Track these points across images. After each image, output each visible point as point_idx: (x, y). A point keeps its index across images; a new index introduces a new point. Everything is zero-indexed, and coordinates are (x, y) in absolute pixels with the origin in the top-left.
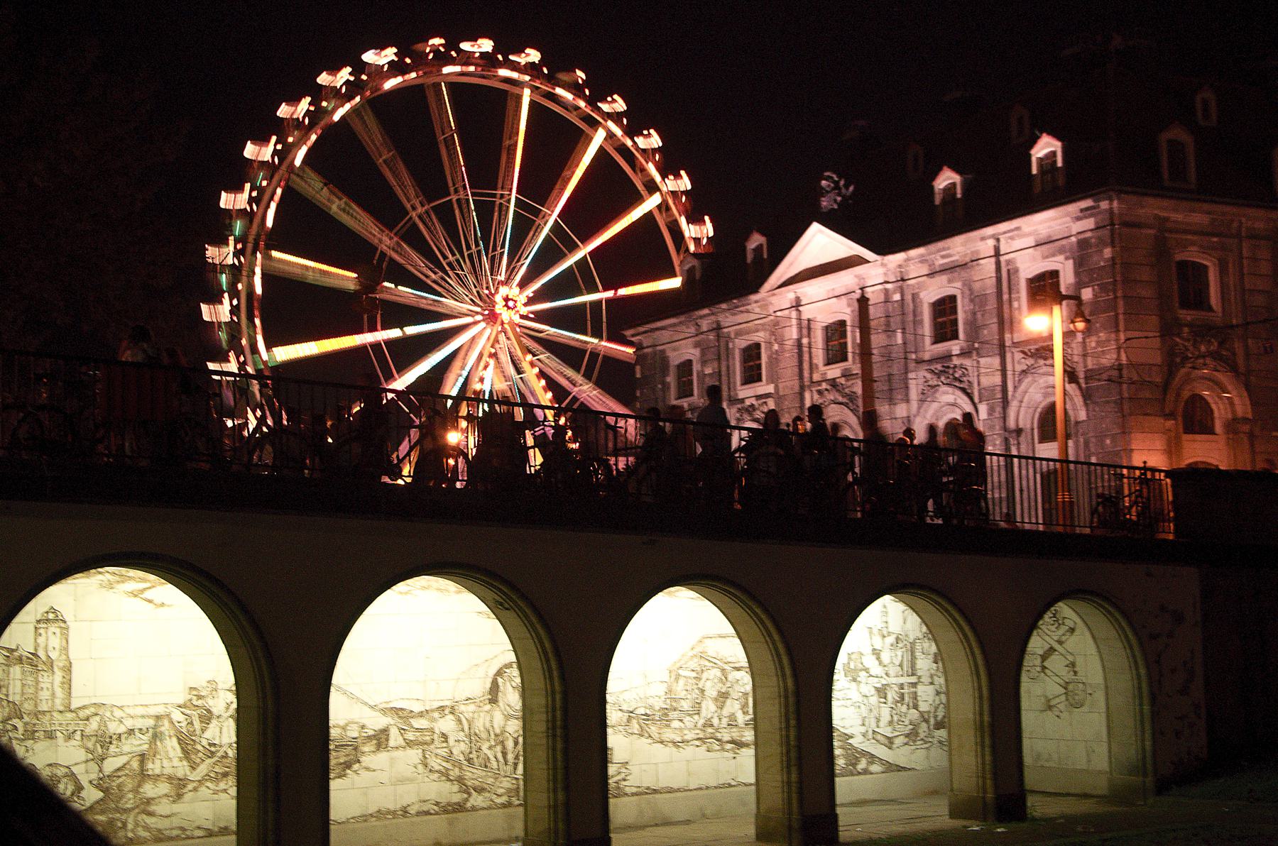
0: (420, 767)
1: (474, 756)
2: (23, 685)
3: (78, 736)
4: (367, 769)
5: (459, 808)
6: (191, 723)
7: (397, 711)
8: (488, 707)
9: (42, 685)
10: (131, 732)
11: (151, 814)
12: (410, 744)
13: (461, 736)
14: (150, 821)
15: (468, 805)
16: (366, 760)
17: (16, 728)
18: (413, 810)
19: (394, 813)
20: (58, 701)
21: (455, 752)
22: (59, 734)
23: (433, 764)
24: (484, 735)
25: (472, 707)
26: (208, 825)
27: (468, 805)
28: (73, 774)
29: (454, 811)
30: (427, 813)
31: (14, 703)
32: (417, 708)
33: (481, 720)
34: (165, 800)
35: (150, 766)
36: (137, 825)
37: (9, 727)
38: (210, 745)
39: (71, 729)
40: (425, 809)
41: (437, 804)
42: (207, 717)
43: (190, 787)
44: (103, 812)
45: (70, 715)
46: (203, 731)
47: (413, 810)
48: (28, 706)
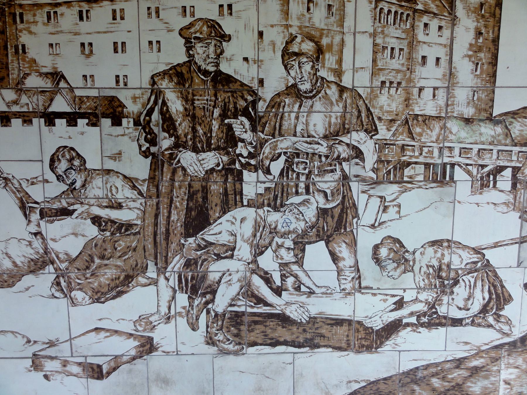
2: (377, 50)
3: (505, 181)
9: (423, 50)
17: (359, 154)
20: (461, 95)
22: (459, 174)
28: (488, 264)
31: (353, 90)
37: (343, 151)
39: (491, 162)
45: (488, 131)
48: (387, 103)
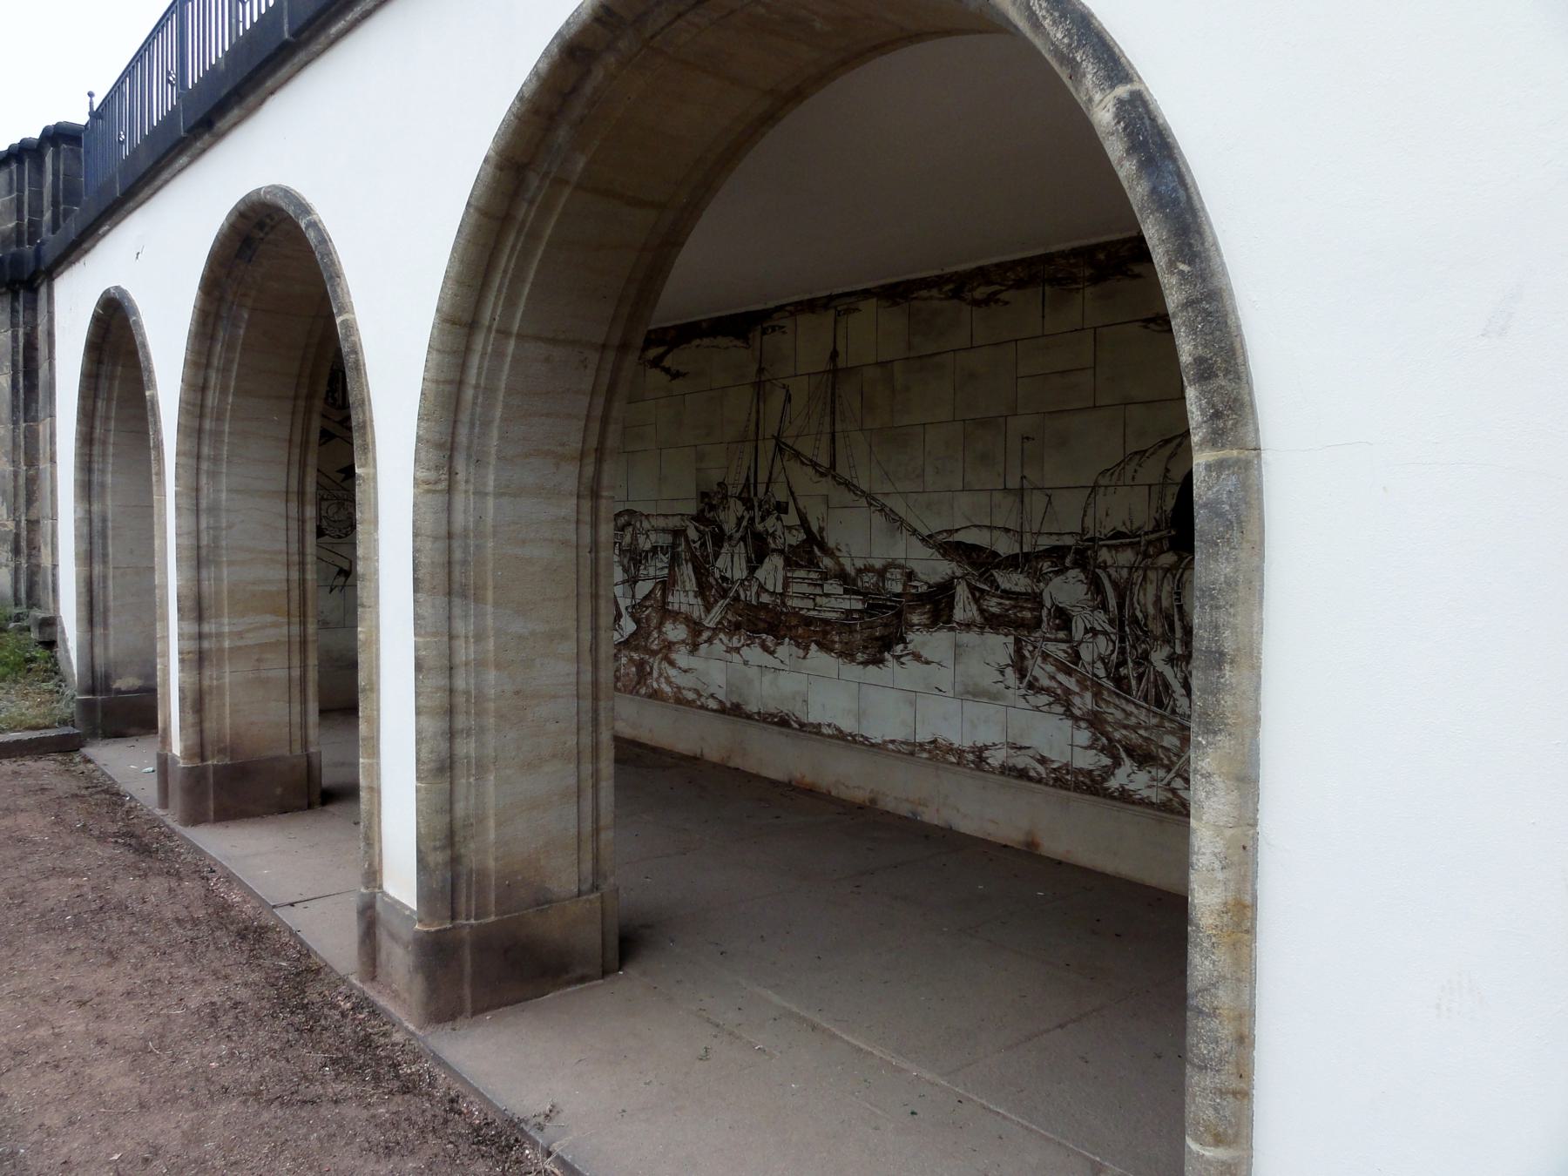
0: (1009, 671)
1: (1129, 670)
4: (917, 657)
5: (1092, 785)
6: (703, 545)
7: (953, 550)
8: (1168, 559)
10: (654, 549)
11: (672, 663)
12: (992, 622)
13: (1100, 620)
14: (672, 672)
15: (1113, 784)
16: (916, 639)
18: (996, 758)
19: (960, 753)
21: (1086, 655)
23: (1037, 672)
24: (1157, 628)
25: (1126, 557)
26: (721, 695)
27: (1113, 784)
29: (1077, 787)
30: (1022, 774)
32: (1005, 546)
33: (1151, 589)
34: (683, 649)
35: (670, 599)
36: (660, 675)
38: (724, 579)
40: (1021, 761)
41: (1043, 761)
42: (719, 539)
43: (705, 635)
44: (636, 649)
46: (716, 557)
47: (996, 758)
